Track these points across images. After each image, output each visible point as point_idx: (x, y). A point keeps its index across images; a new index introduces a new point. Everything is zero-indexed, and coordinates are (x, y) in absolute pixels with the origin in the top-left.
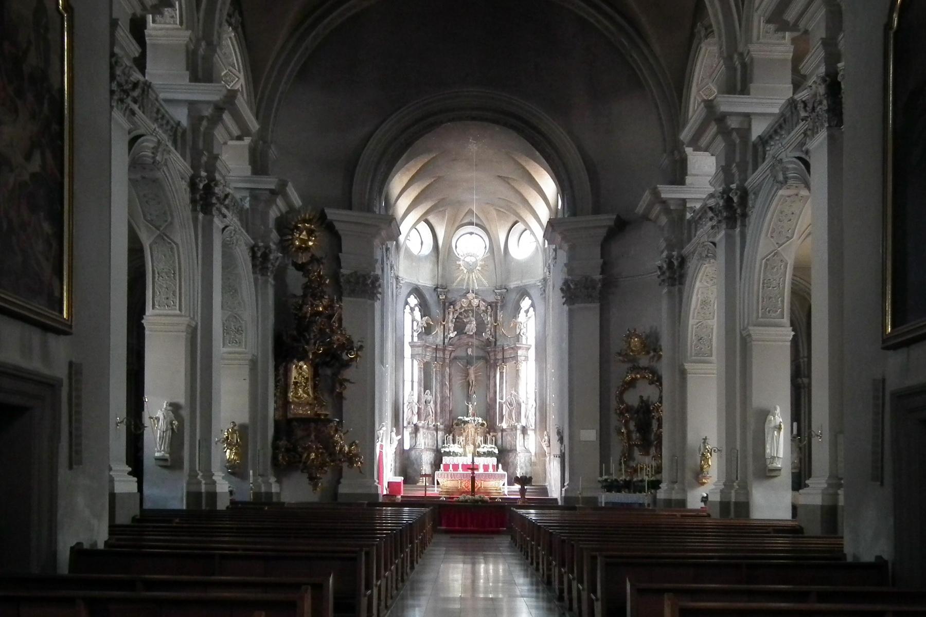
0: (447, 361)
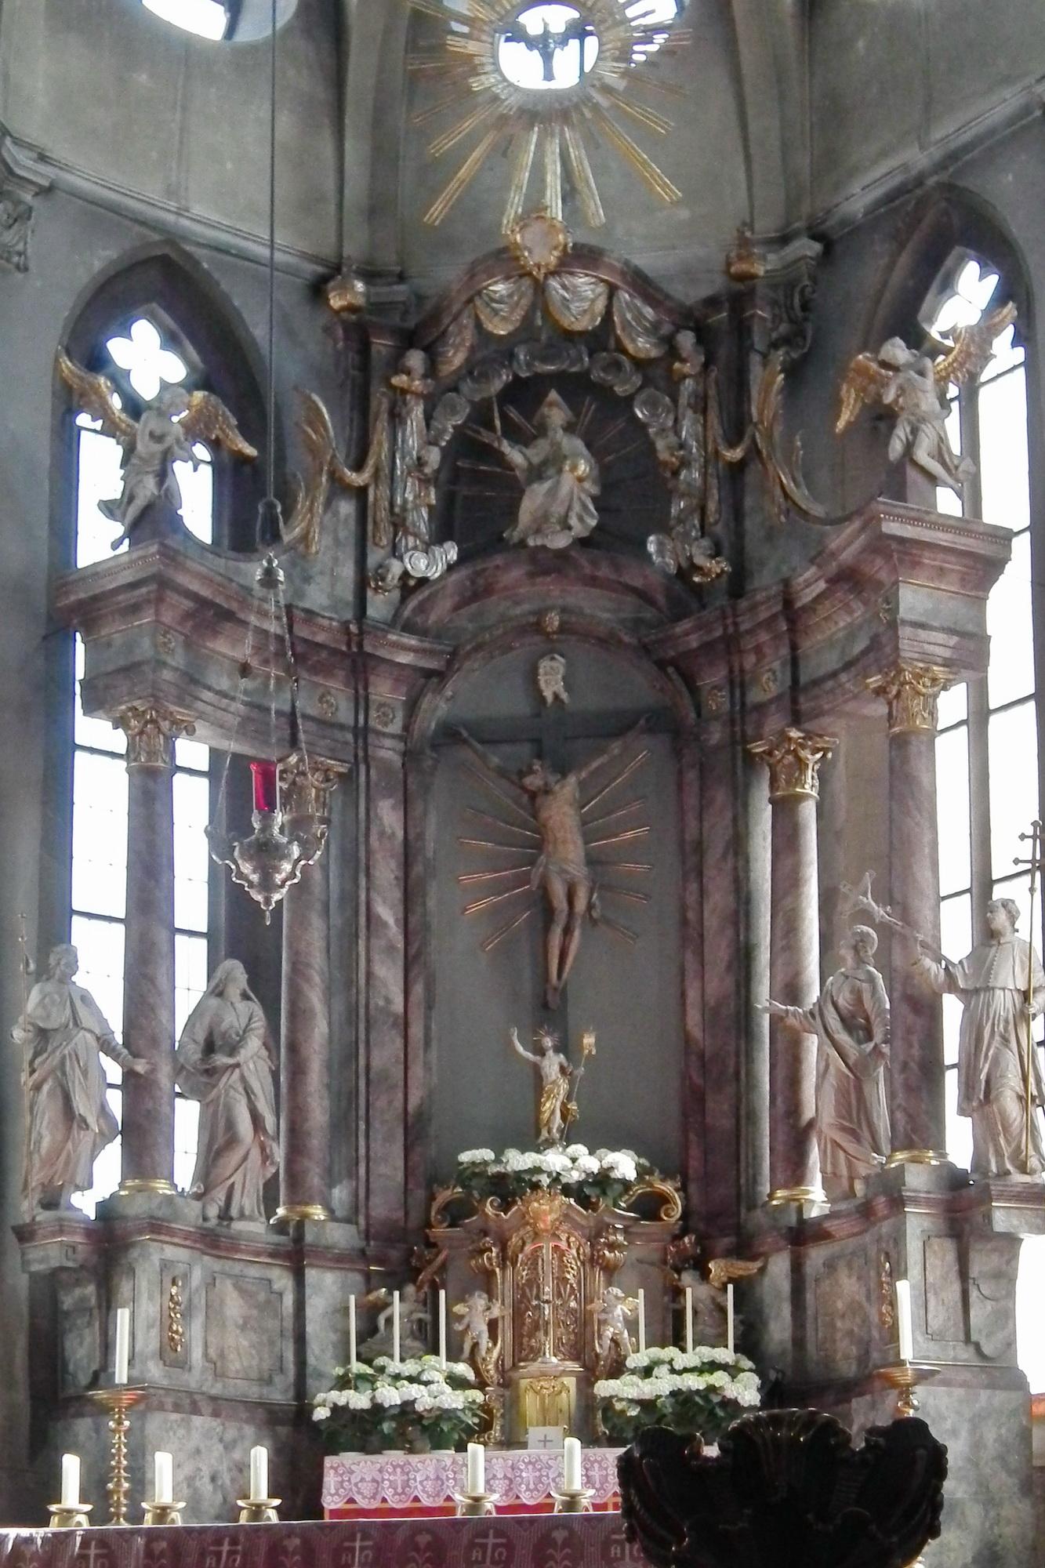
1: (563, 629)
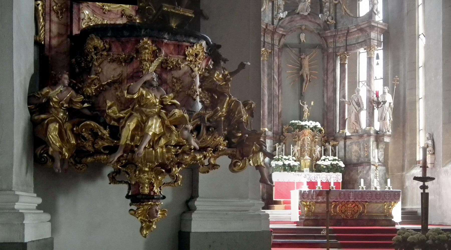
0: (276, 49)
1: (305, 29)
